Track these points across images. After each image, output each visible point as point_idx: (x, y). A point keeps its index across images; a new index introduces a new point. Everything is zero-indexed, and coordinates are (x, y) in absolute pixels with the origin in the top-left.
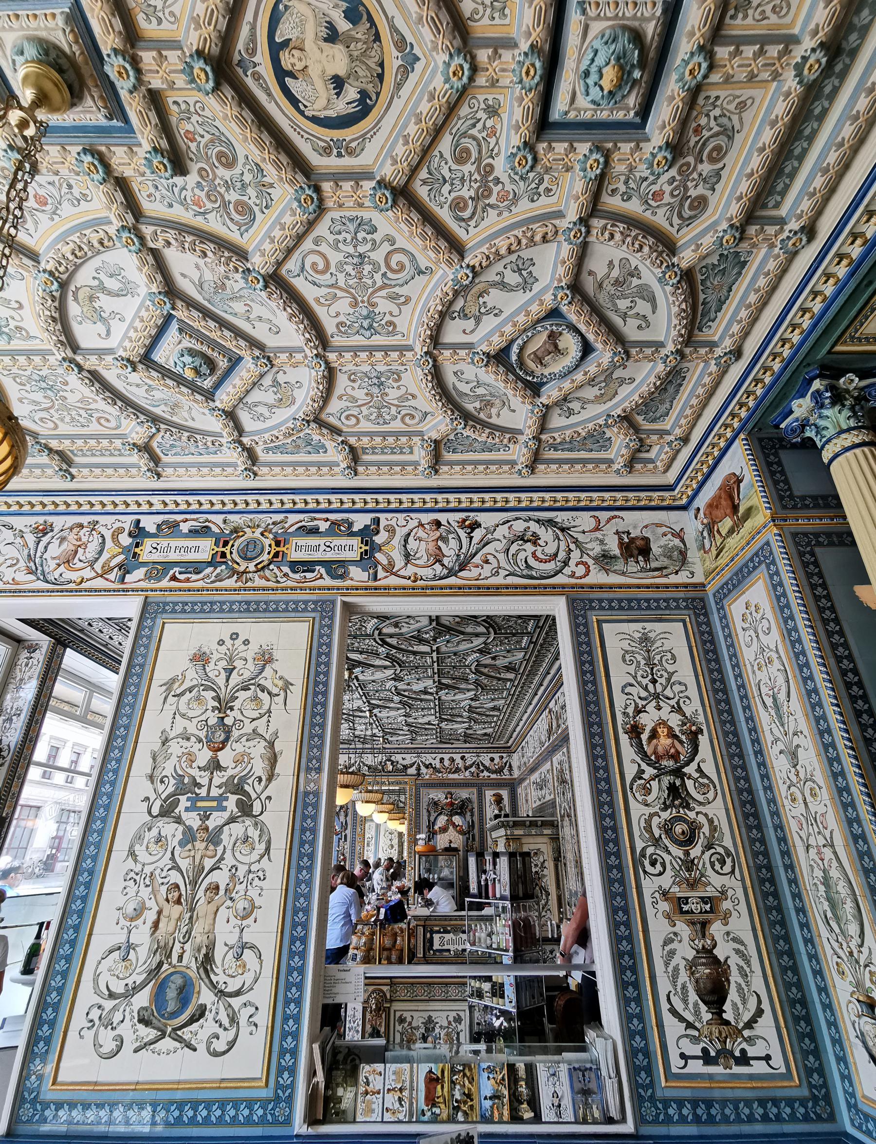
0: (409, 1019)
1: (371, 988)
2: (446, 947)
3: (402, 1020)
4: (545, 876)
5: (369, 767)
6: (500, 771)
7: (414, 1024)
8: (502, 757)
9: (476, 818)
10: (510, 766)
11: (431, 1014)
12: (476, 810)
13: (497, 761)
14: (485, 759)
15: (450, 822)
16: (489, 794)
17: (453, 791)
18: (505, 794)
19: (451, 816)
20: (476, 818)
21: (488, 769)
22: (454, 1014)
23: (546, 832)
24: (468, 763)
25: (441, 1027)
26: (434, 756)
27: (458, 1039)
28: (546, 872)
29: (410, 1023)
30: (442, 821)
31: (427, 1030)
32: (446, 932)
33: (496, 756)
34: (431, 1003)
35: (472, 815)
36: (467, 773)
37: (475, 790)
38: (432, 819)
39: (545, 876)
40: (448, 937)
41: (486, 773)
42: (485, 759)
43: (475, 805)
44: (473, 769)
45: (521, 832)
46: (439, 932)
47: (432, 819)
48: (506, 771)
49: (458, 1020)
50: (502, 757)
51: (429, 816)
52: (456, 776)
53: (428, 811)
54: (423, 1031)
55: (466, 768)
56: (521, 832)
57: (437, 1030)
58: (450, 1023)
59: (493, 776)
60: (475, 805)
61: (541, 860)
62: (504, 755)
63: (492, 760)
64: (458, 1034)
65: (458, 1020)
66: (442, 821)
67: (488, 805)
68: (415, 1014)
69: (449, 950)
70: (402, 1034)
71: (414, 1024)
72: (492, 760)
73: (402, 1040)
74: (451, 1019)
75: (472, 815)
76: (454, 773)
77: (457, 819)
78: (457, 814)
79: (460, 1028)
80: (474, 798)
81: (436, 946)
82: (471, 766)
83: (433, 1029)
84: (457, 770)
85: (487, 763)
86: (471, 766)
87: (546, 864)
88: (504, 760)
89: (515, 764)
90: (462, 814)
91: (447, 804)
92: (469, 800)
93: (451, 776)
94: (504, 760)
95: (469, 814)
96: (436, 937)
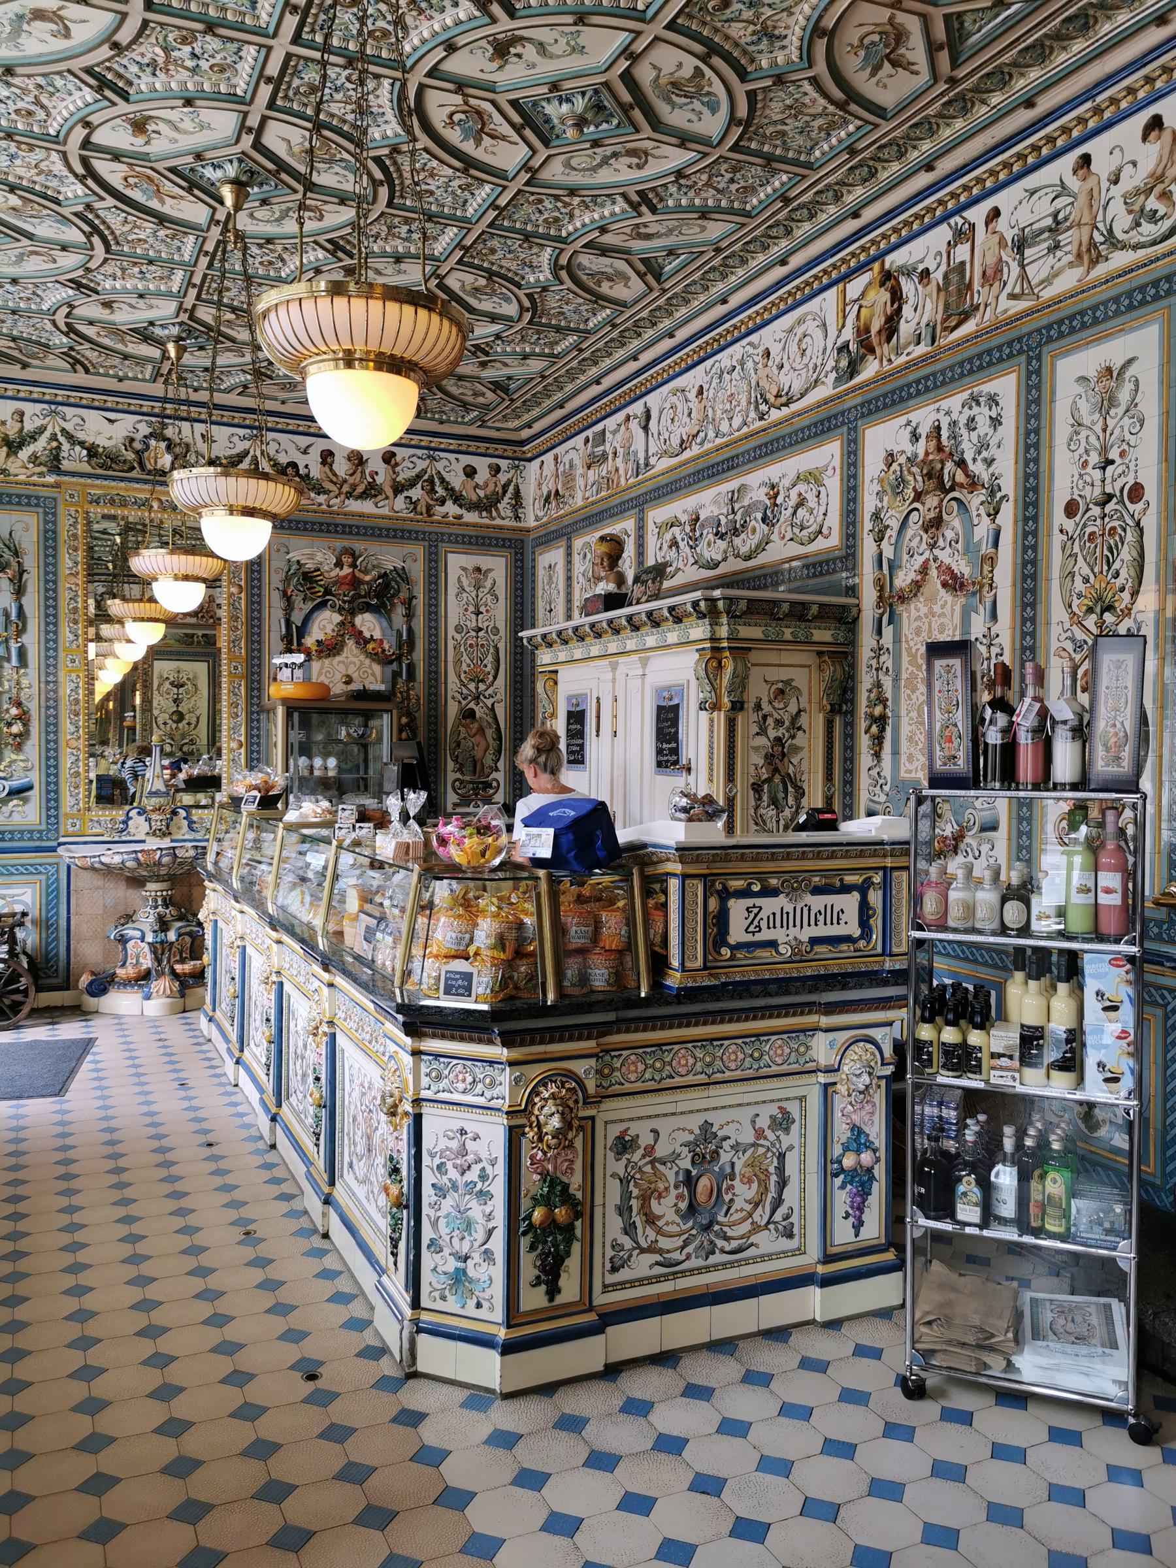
0: (646, 1139)
1: (535, 1072)
2: (766, 935)
3: (624, 1145)
4: (796, 749)
5: (92, 451)
6: (488, 505)
7: (661, 1151)
8: (496, 470)
9: (419, 624)
10: (517, 494)
11: (710, 1117)
12: (420, 603)
13: (483, 476)
14: (452, 469)
15: (347, 628)
16: (457, 563)
17: (358, 546)
18: (497, 566)
19: (353, 613)
20: (419, 624)
21: (457, 499)
22: (773, 1109)
23: (822, 635)
24: (404, 475)
25: (736, 1147)
26: (303, 441)
27: (781, 1169)
28: (800, 739)
29: (650, 1150)
30: (325, 624)
31: (698, 1159)
32: (769, 892)
33: (482, 464)
34: (714, 1091)
35: (409, 615)
36: (400, 503)
37: (419, 550)
38: (297, 618)
39: (796, 749)
40: (770, 905)
41: (451, 508)
42: (452, 469)
43: (420, 591)
44: (416, 493)
45: (756, 632)
46: (745, 893)
47: (297, 618)
48: (504, 506)
49: (783, 1122)
50: (496, 470)
51: (289, 608)
52: (366, 507)
53: (285, 594)
54: (686, 1163)
55: (398, 489)
56: (756, 632)
57: (725, 1157)
58: (760, 1134)
59: (471, 517)
60: (420, 591)
61: (793, 708)
62: (504, 464)
63: (470, 472)
64: (782, 1157)
65: (783, 1122)
66: (325, 624)
67: (452, 590)
68: (663, 1125)
69: (773, 944)
70: (624, 1181)
71: (661, 1151)
72: (470, 472)
73: (626, 1196)
74: (763, 1122)
75: (409, 615)
76: (364, 496)
77: (368, 623)
78: (368, 608)
79: (786, 1140)
80: (417, 571)
81: (737, 933)
82: (412, 483)
83: (715, 1155)
84: (371, 491)
85: (457, 480)
86: (412, 483)
87: (803, 720)
88: (503, 478)
89: (530, 491)
90: (381, 608)
91: (339, 581)
92: (403, 575)
93: (355, 506)
94: (503, 478)
95: (400, 610)
96: (737, 908)
